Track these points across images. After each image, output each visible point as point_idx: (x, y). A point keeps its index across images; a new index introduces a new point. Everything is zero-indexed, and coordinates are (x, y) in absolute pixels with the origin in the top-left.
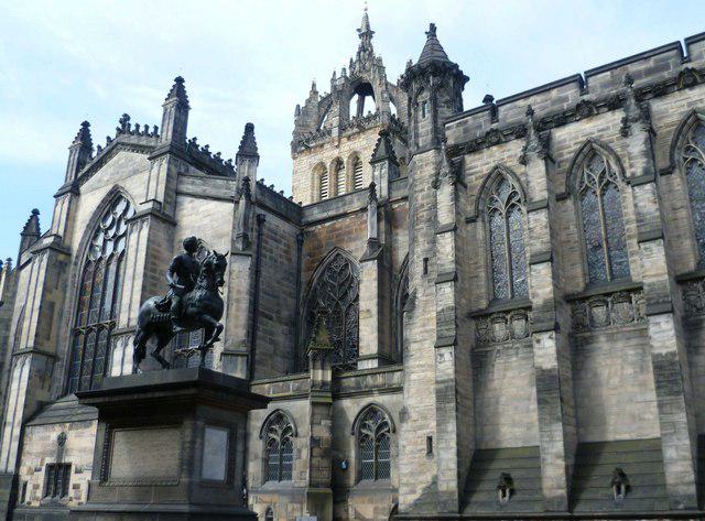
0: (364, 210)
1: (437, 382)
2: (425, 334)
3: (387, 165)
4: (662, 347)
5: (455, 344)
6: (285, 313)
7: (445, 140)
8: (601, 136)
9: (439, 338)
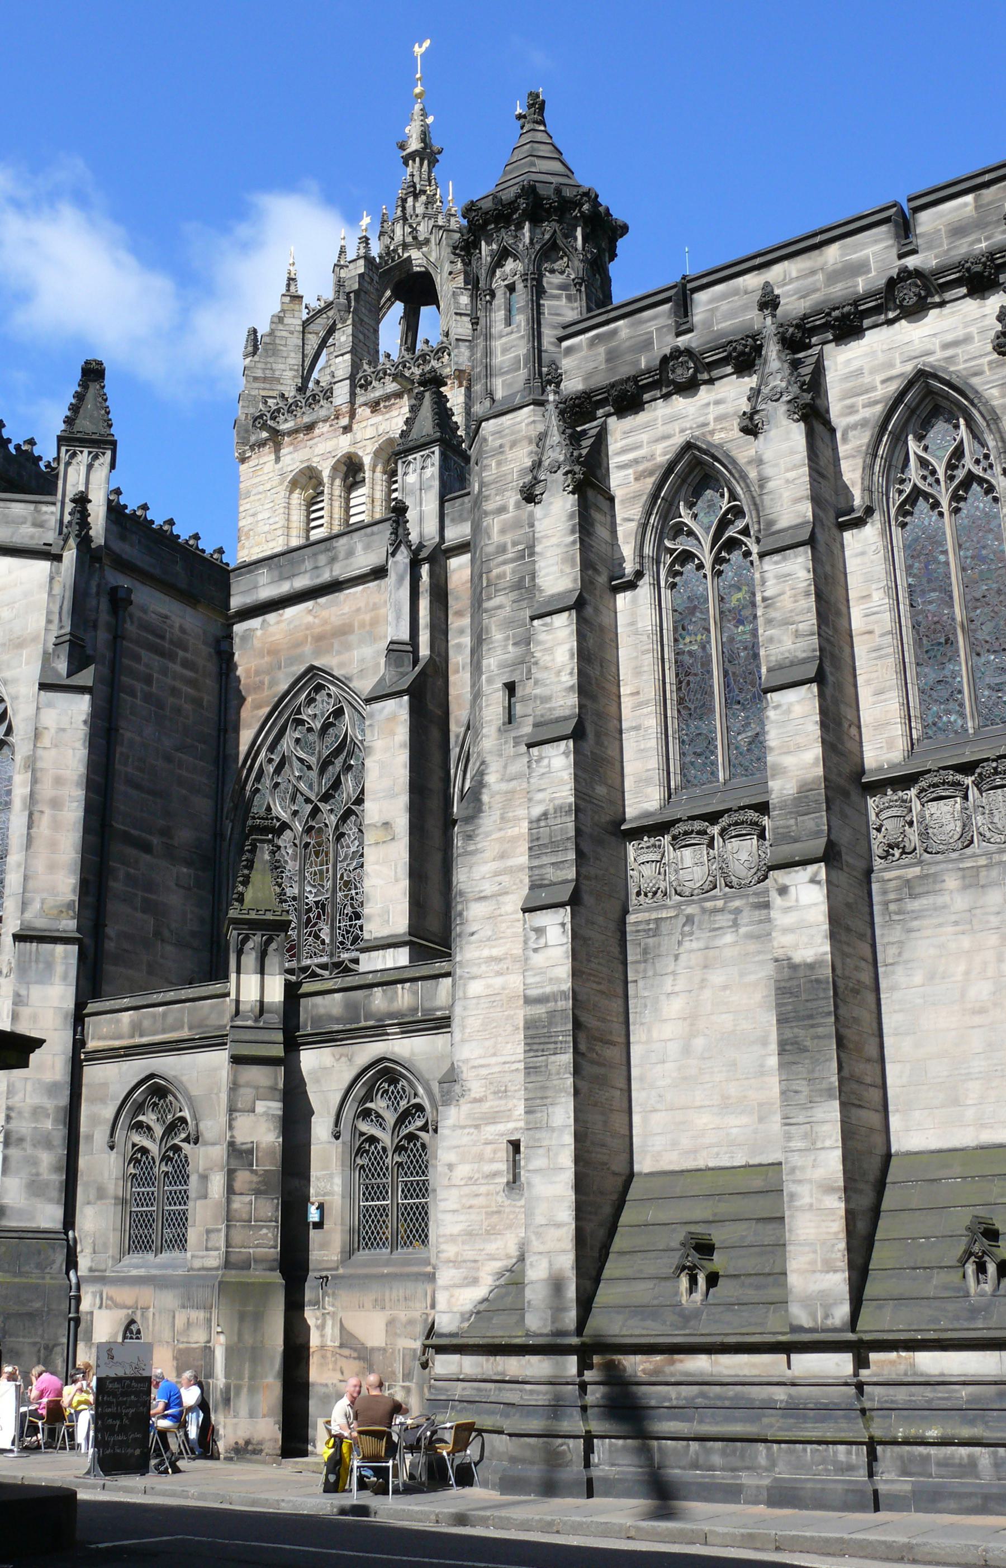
0: (379, 573)
1: (528, 1001)
2: (505, 879)
3: (436, 458)
5: (575, 901)
6: (184, 836)
7: (556, 380)
8: (950, 359)
9: (534, 887)
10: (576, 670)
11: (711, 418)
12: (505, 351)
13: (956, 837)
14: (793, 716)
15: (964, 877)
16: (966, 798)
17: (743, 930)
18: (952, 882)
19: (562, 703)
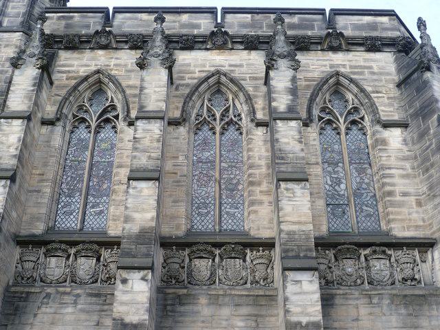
4: (302, 313)
10: (20, 148)
11: (112, 64)
12: (13, 8)
13: (206, 279)
14: (142, 194)
15: (210, 299)
16: (213, 260)
17: (79, 306)
18: (203, 300)
19: (7, 162)
